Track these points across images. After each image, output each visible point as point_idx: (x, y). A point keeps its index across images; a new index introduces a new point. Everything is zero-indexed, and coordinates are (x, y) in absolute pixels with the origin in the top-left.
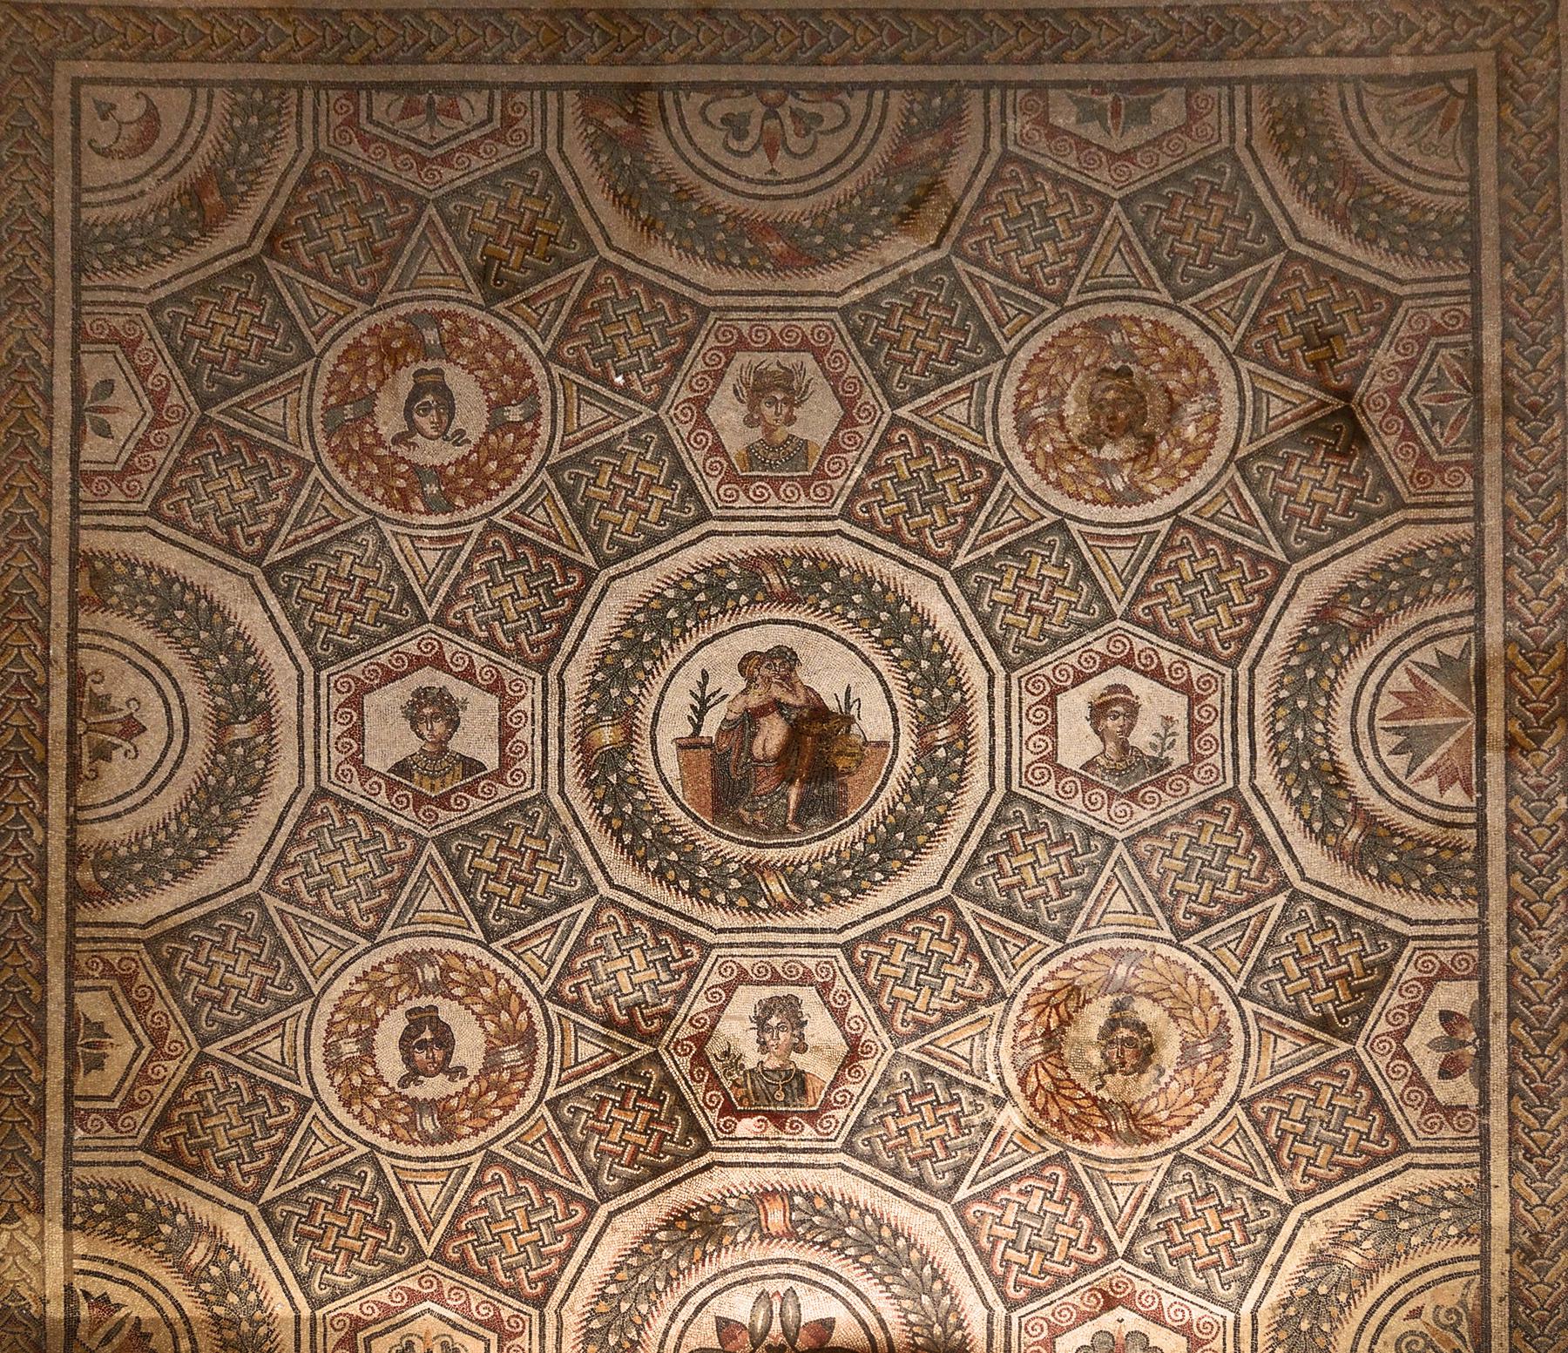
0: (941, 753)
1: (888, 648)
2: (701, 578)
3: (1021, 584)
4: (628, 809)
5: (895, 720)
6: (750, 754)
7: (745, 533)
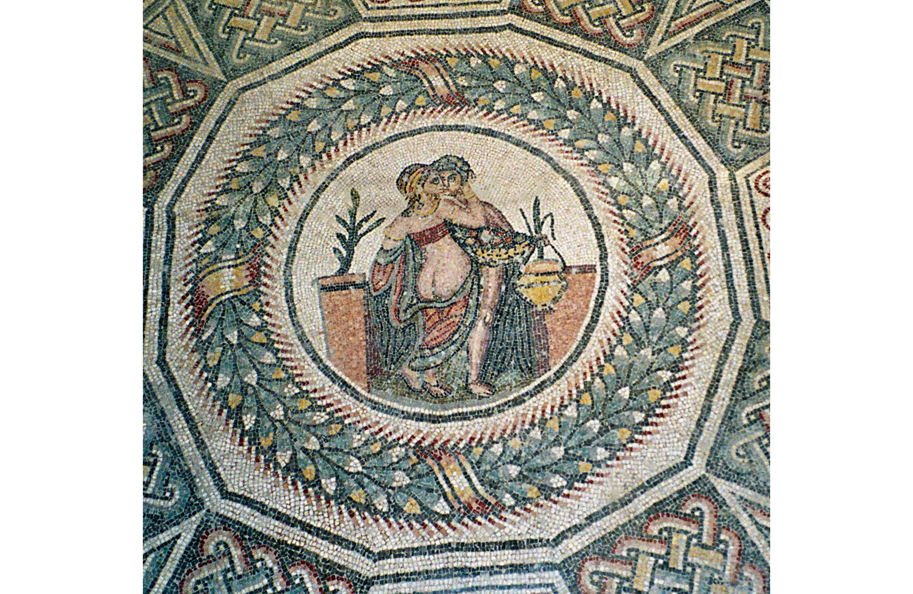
0: (664, 275)
1: (582, 151)
2: (349, 84)
3: (728, 70)
4: (252, 378)
5: (600, 237)
6: (415, 289)
7: (401, 33)
